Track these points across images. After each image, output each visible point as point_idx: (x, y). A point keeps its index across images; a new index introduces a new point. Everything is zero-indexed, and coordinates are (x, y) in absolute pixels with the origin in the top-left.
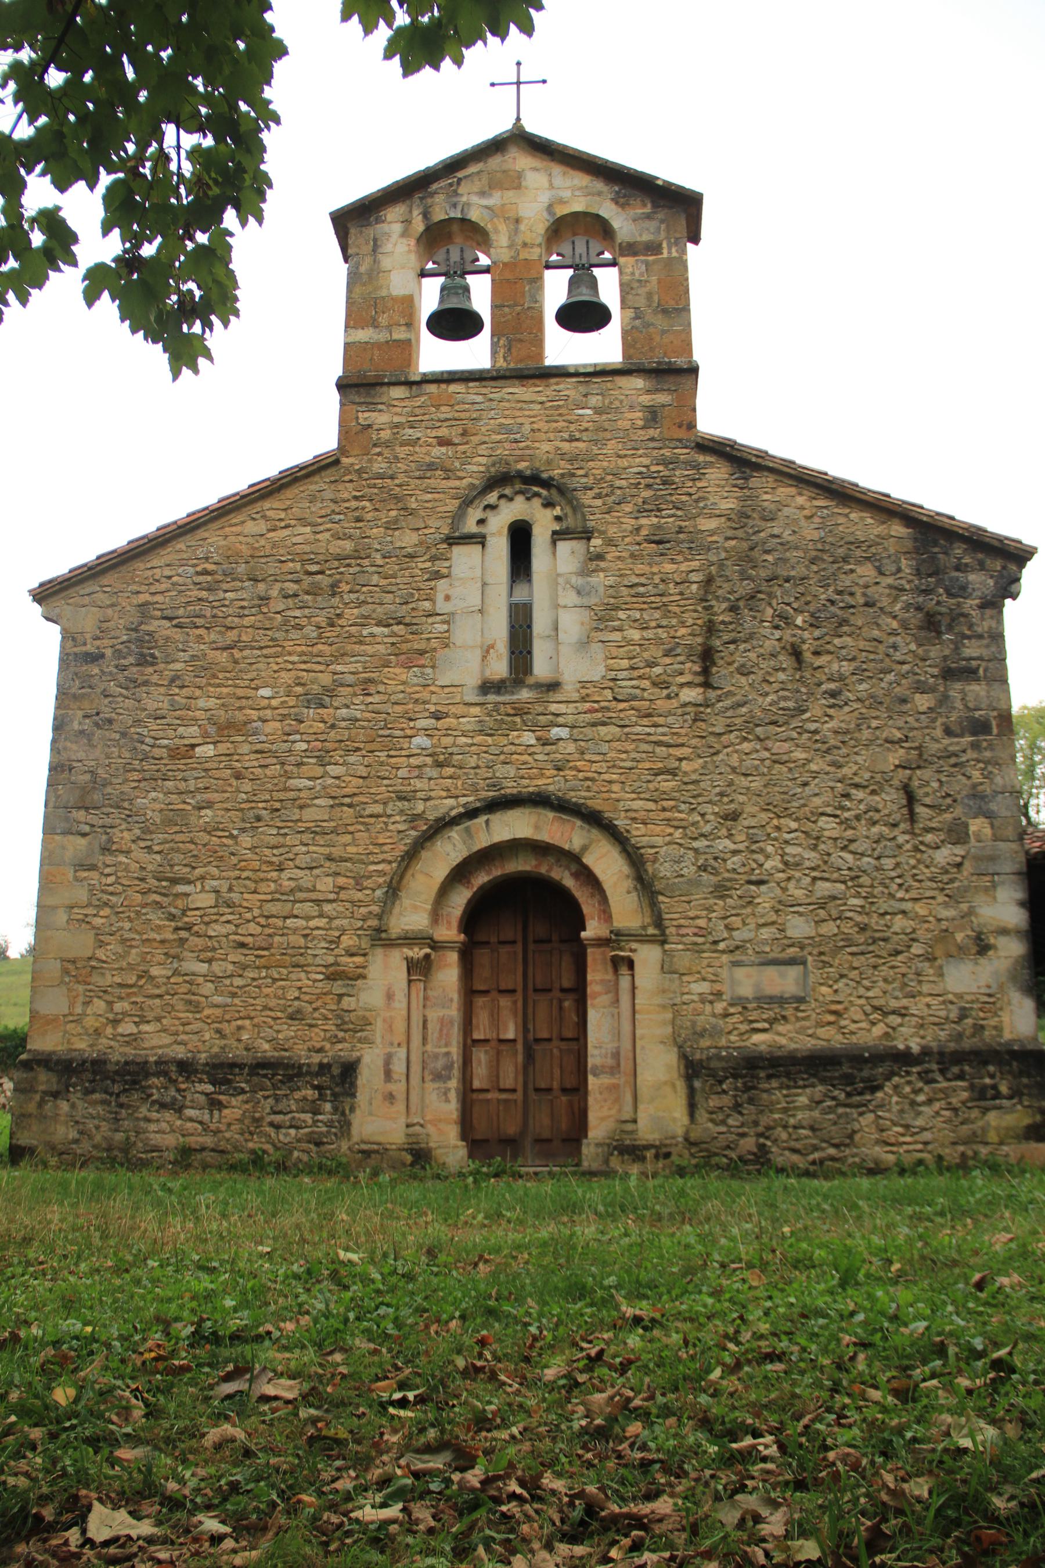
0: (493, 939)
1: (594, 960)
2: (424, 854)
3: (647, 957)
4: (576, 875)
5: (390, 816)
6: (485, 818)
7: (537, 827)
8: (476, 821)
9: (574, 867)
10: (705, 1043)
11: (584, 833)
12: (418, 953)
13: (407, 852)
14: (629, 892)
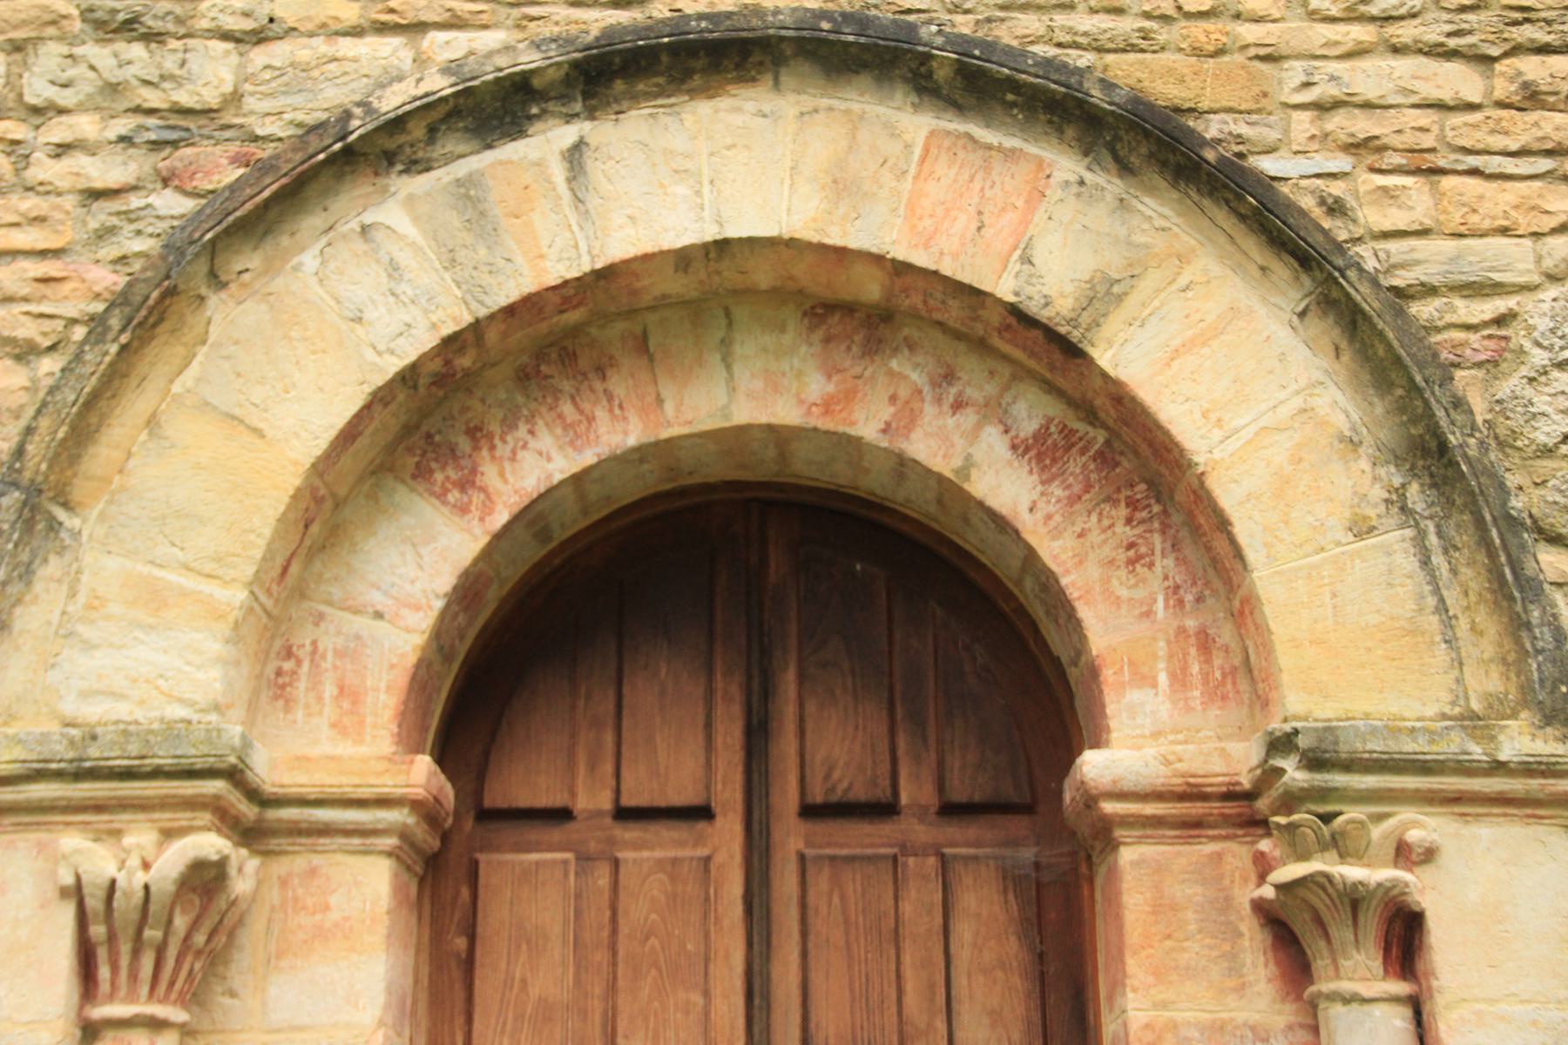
0: (592, 798)
1: (1162, 908)
2: (226, 315)
4: (1042, 452)
5: (39, 112)
6: (566, 134)
7: (841, 186)
8: (511, 151)
9: (1031, 411)
11: (1100, 216)
12: (144, 857)
13: (121, 300)
14: (1362, 529)
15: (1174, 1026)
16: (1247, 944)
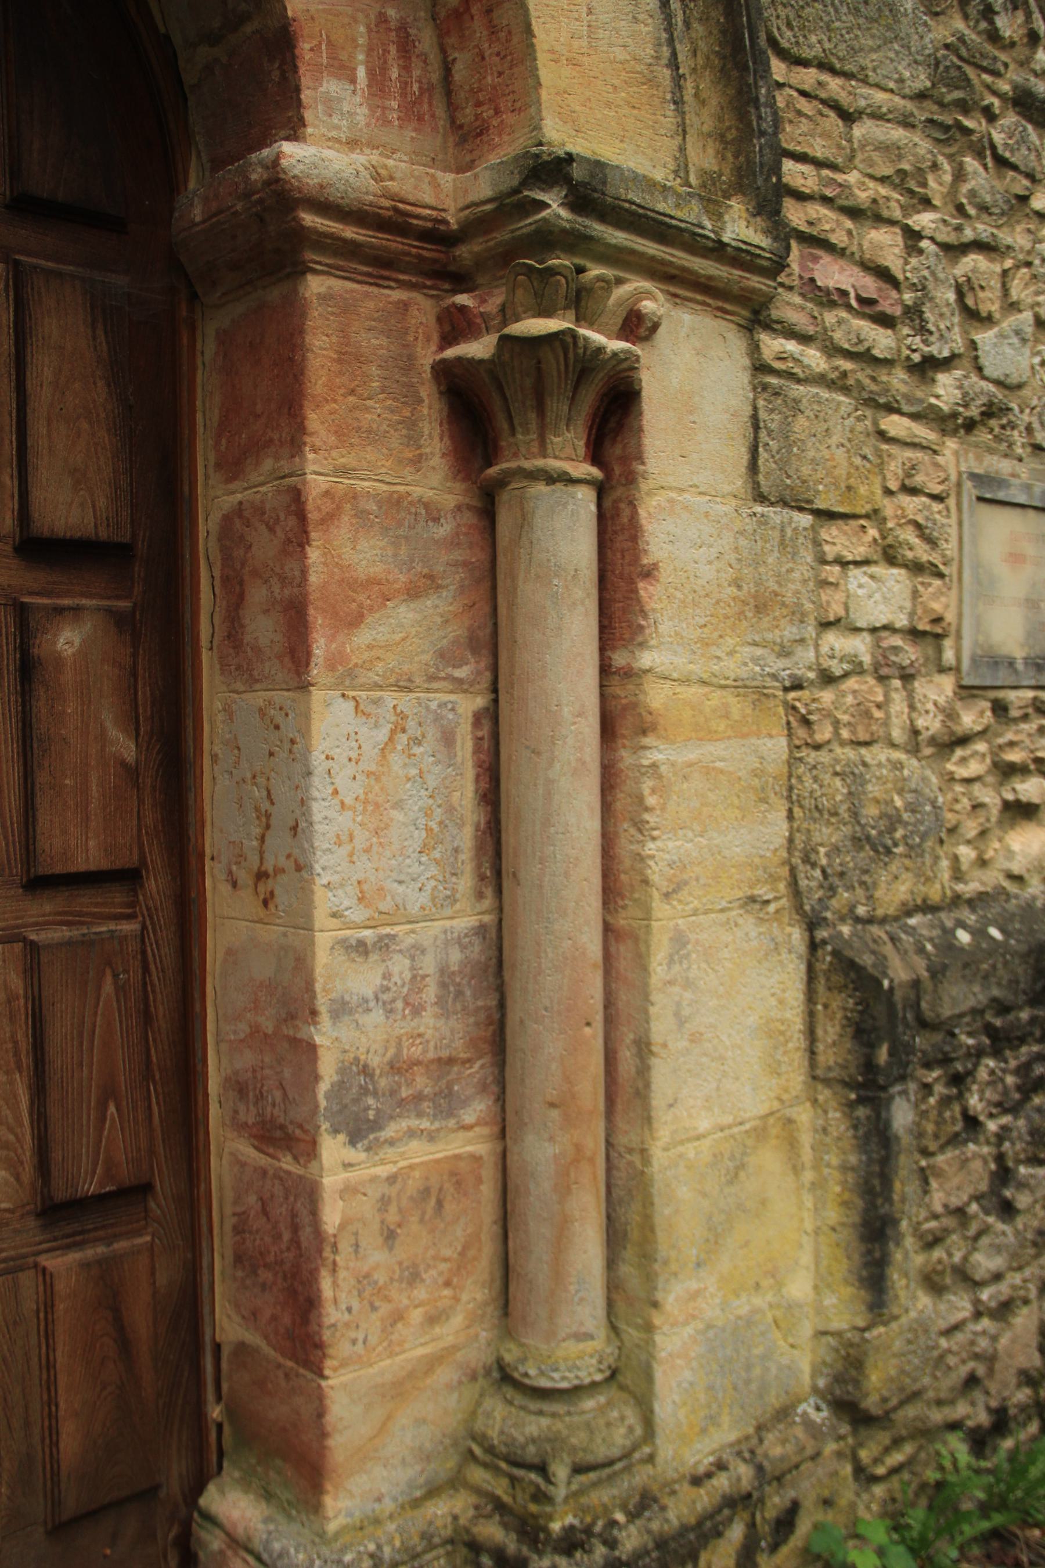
1: (348, 357)
3: (692, 376)
10: (895, 888)
15: (354, 496)
16: (426, 411)
